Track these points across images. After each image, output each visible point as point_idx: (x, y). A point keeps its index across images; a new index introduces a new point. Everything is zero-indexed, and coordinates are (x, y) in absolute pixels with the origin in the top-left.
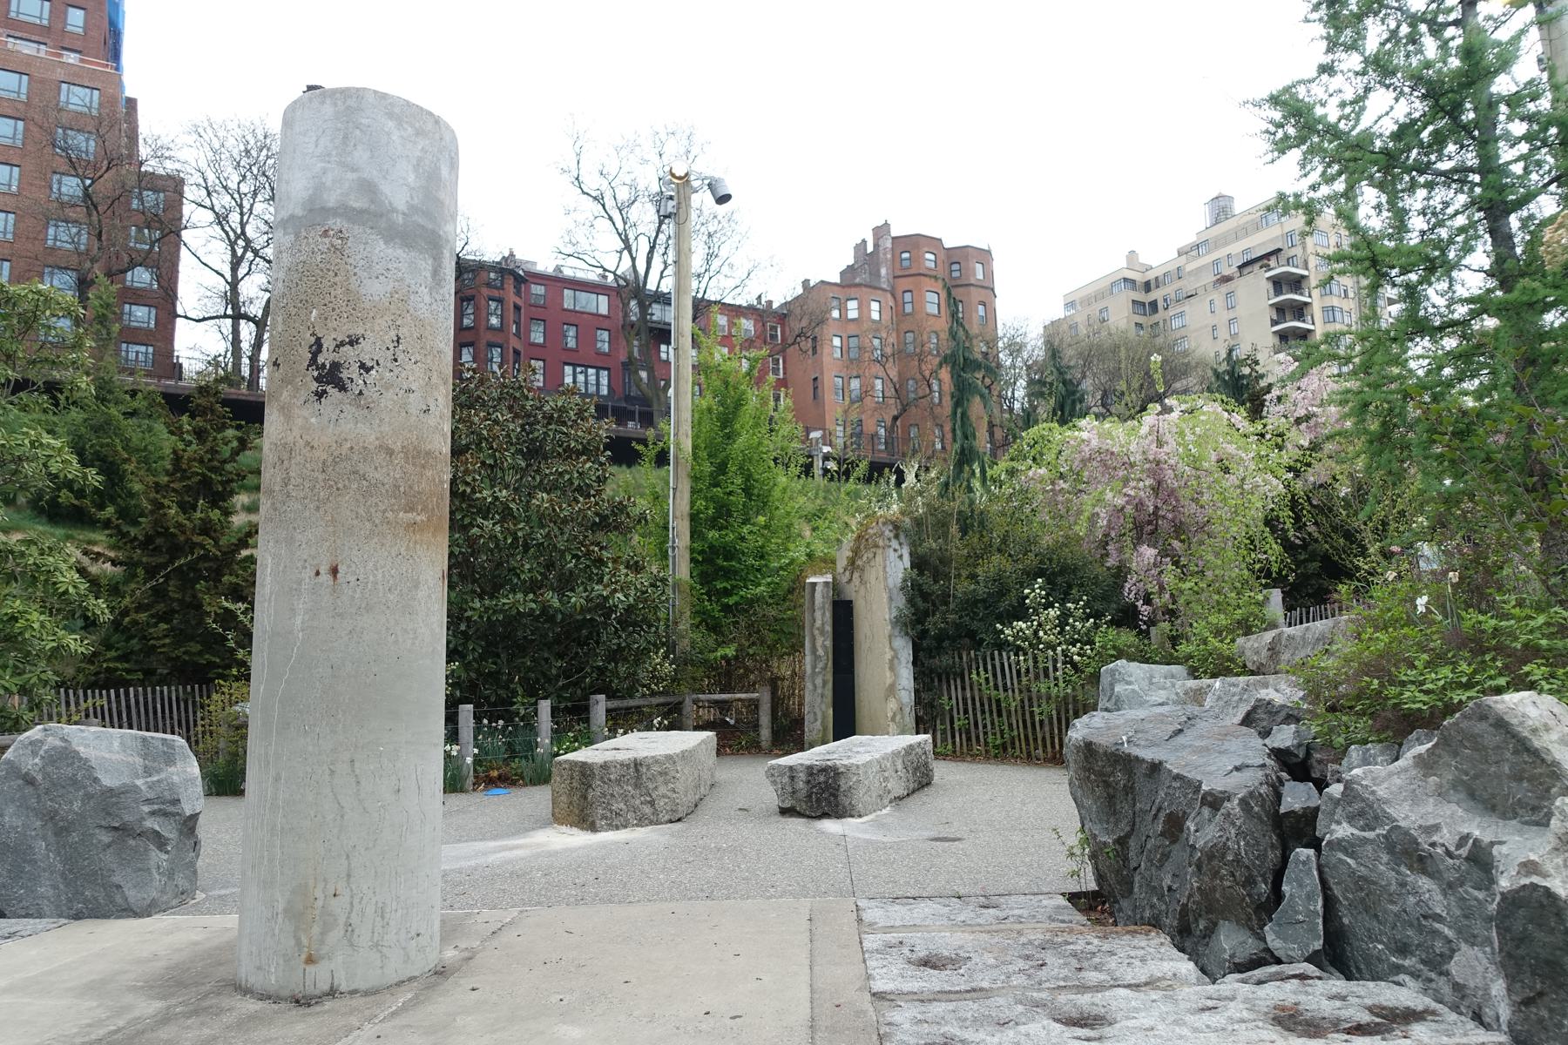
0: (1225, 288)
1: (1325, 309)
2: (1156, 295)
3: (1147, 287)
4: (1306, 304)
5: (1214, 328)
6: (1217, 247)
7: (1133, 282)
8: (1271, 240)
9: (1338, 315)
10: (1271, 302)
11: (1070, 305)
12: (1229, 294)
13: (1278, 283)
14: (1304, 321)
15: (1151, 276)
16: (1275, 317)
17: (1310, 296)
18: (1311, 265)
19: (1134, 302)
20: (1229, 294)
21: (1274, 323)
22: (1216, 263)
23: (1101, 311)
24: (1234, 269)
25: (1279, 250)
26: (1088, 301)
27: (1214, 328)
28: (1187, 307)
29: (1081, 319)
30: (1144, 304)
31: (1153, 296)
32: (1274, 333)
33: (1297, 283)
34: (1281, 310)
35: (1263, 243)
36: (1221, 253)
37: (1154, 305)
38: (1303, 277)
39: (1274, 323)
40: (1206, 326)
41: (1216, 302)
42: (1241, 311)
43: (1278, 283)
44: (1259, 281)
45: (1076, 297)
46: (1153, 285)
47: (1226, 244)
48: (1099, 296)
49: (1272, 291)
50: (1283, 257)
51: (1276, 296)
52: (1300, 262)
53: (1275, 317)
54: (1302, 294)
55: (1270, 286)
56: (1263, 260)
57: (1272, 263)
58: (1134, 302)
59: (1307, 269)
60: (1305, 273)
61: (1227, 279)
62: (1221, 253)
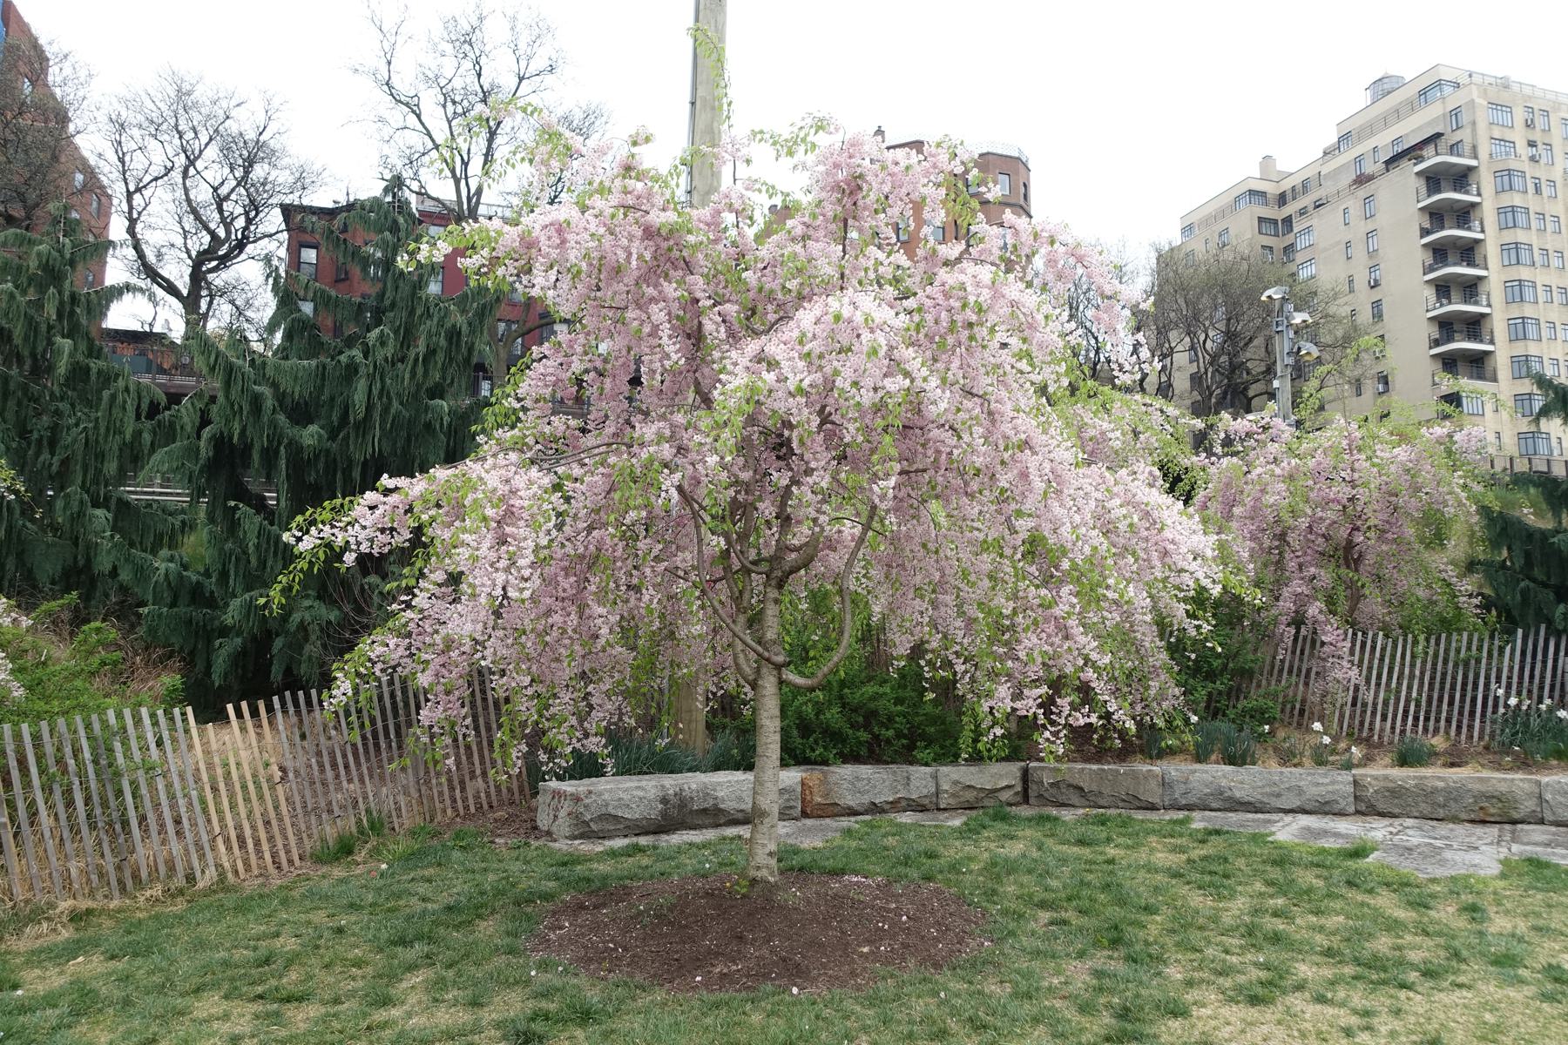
0: (1362, 192)
1: (1501, 211)
2: (1290, 209)
3: (1282, 199)
4: (1474, 205)
5: (1348, 245)
6: (1360, 140)
7: (1263, 194)
8: (1429, 123)
9: (1521, 219)
10: (1421, 205)
11: (1187, 229)
12: (1368, 199)
13: (1434, 180)
14: (1469, 229)
15: (1286, 185)
16: (1427, 225)
17: (1479, 194)
18: (1483, 152)
19: (1260, 219)
20: (1368, 199)
21: (1425, 232)
22: (1358, 160)
23: (1220, 235)
24: (1380, 166)
25: (1438, 135)
26: (1207, 221)
27: (1348, 245)
28: (1316, 220)
29: (1198, 246)
30: (1275, 222)
31: (1290, 209)
32: (1425, 246)
33: (1462, 178)
34: (1437, 216)
35: (1419, 128)
36: (1365, 147)
37: (1288, 221)
38: (1470, 169)
39: (1425, 232)
40: (1338, 243)
41: (1351, 211)
42: (1382, 220)
43: (1434, 180)
44: (1408, 175)
45: (1194, 219)
46: (1289, 196)
47: (1372, 134)
48: (1221, 214)
49: (1423, 190)
50: (1443, 144)
51: (1429, 196)
52: (1467, 149)
53: (1427, 225)
54: (1467, 192)
55: (1421, 184)
56: (1412, 152)
57: (1429, 151)
58: (1260, 219)
59: (1476, 157)
60: (1473, 163)
61: (1362, 180)
62: (1365, 147)
